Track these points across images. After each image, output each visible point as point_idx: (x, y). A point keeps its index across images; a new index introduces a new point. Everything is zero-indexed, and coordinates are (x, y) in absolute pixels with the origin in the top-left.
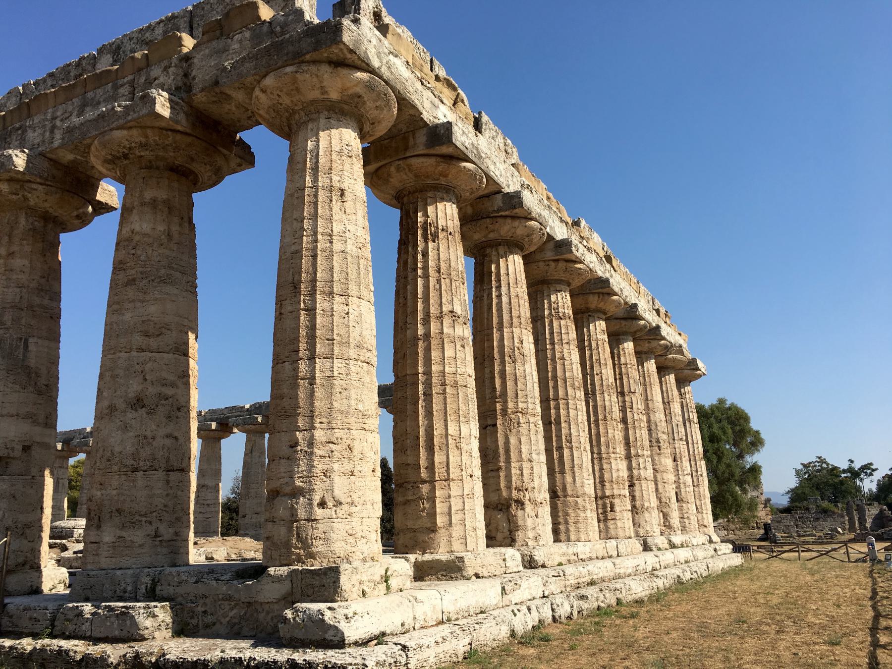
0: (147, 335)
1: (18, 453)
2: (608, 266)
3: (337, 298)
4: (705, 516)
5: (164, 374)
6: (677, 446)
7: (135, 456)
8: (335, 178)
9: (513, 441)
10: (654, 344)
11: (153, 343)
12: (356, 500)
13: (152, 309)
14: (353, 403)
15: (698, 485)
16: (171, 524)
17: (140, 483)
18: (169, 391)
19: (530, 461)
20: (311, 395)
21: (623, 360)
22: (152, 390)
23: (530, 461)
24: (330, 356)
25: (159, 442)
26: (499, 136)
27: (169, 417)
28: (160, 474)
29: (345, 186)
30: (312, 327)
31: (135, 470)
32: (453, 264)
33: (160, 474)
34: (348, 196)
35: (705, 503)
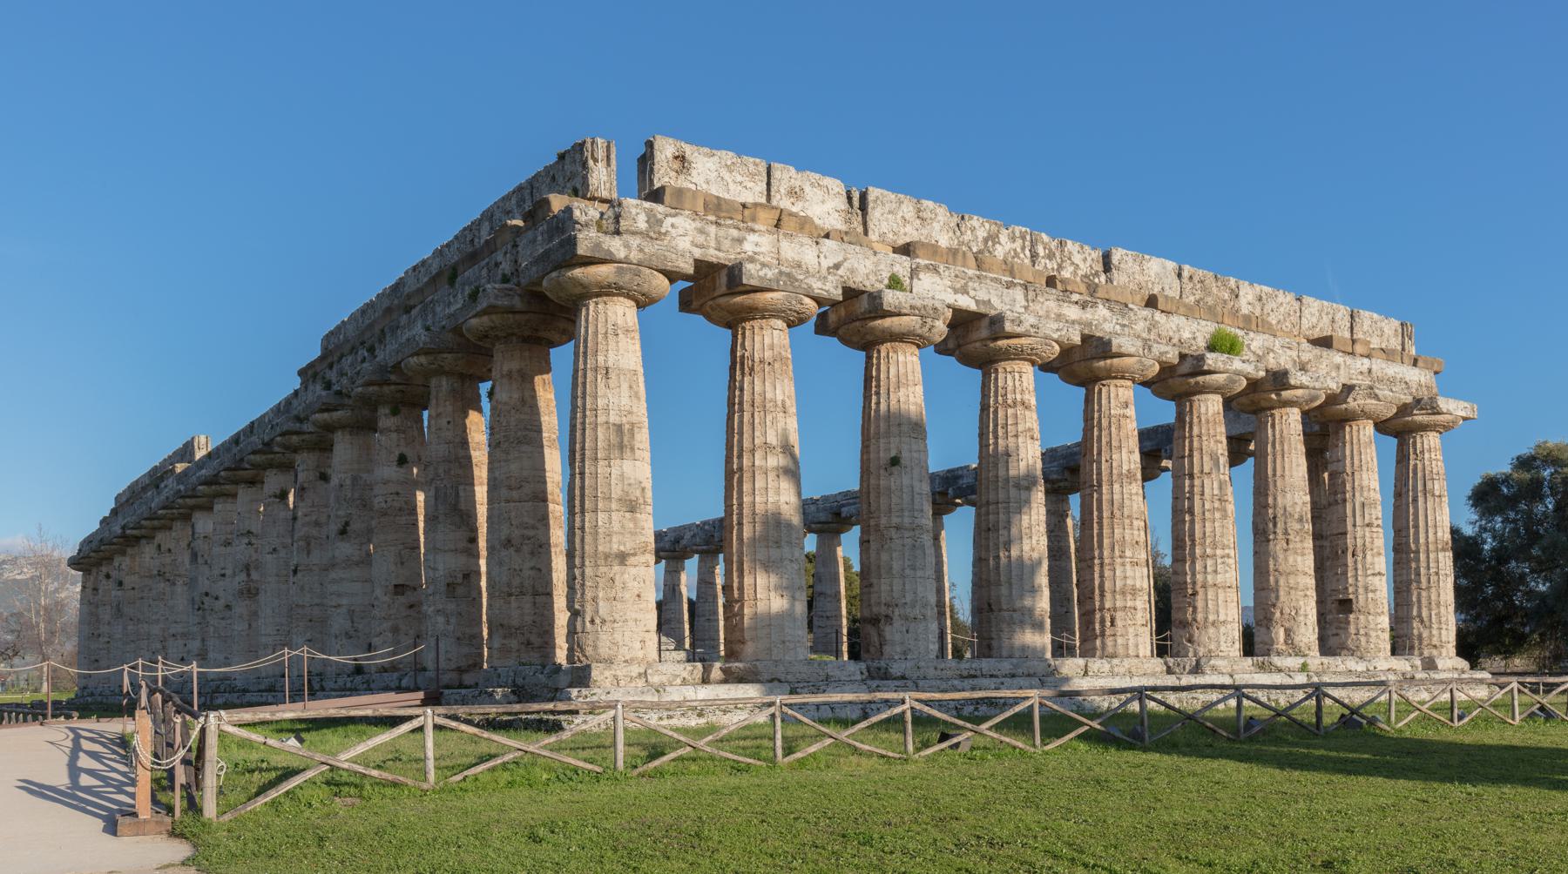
0: (510, 488)
1: (460, 580)
2: (1147, 312)
3: (601, 463)
4: (1435, 632)
5: (526, 519)
6: (1359, 535)
7: (509, 585)
8: (601, 359)
9: (884, 557)
10: (1286, 394)
11: (515, 494)
12: (617, 617)
13: (513, 466)
14: (615, 546)
15: (1429, 588)
16: (540, 636)
17: (514, 605)
18: (531, 533)
19: (903, 577)
20: (583, 540)
21: (1196, 431)
22: (516, 533)
23: (903, 577)
24: (595, 511)
25: (527, 573)
26: (904, 207)
27: (532, 553)
28: (528, 598)
29: (610, 364)
30: (582, 488)
31: (510, 595)
32: (769, 395)
33: (528, 598)
34: (612, 375)
35: (1438, 614)
